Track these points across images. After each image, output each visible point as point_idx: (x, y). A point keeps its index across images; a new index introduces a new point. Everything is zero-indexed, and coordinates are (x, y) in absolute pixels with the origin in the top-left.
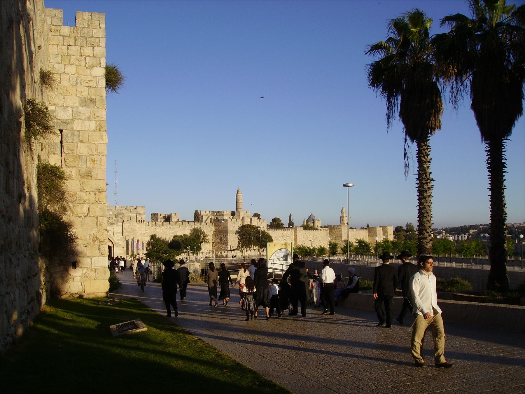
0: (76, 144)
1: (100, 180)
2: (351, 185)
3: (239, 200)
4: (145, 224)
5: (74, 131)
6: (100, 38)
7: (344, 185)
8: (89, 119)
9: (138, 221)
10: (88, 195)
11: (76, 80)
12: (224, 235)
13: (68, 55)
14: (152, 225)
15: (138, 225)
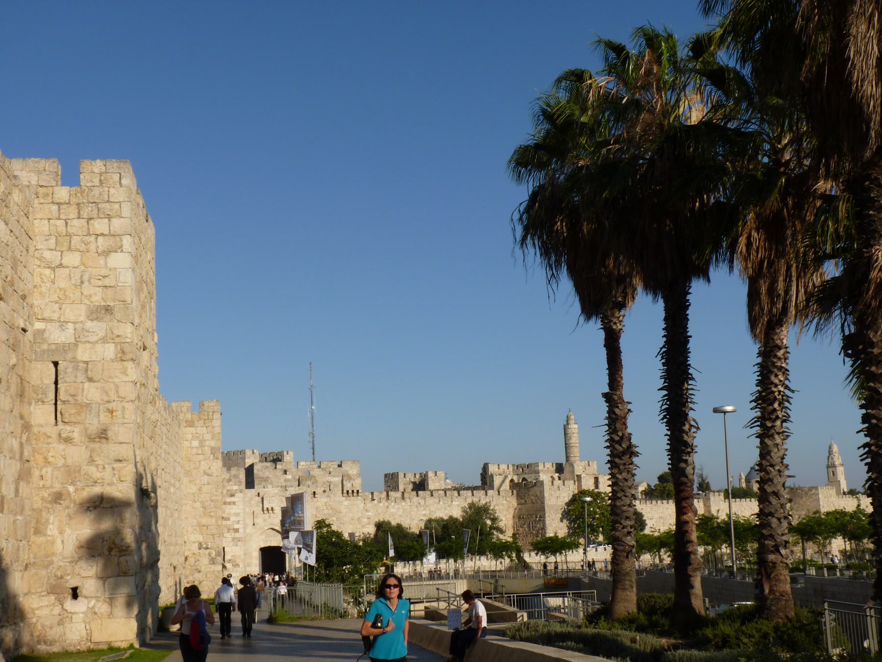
0: (81, 384)
1: (121, 443)
2: (729, 408)
3: (570, 439)
4: (359, 498)
5: (78, 362)
6: (120, 202)
7: (716, 411)
8: (104, 340)
9: (345, 491)
10: (101, 470)
11: (81, 277)
12: (536, 517)
13: (66, 235)
14: (380, 499)
15: (346, 500)
